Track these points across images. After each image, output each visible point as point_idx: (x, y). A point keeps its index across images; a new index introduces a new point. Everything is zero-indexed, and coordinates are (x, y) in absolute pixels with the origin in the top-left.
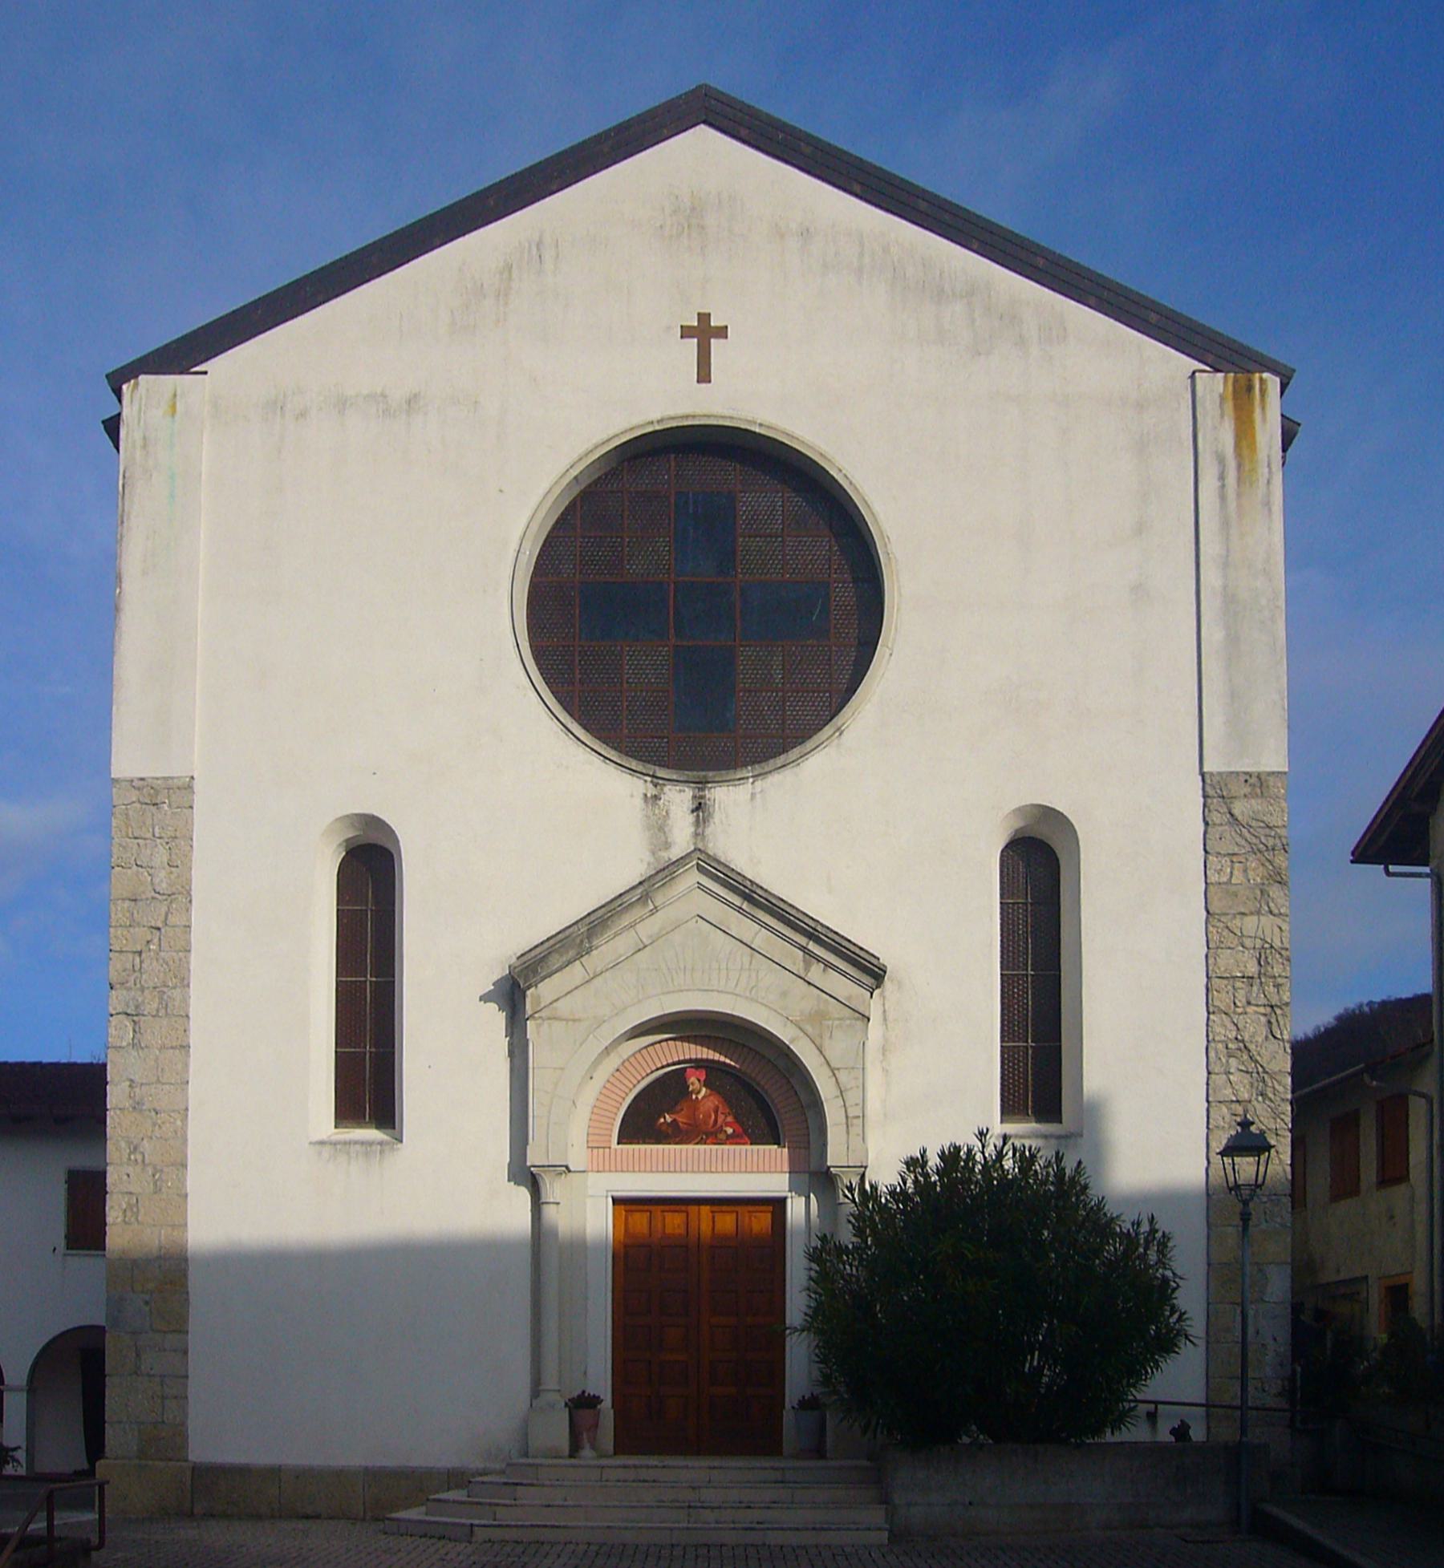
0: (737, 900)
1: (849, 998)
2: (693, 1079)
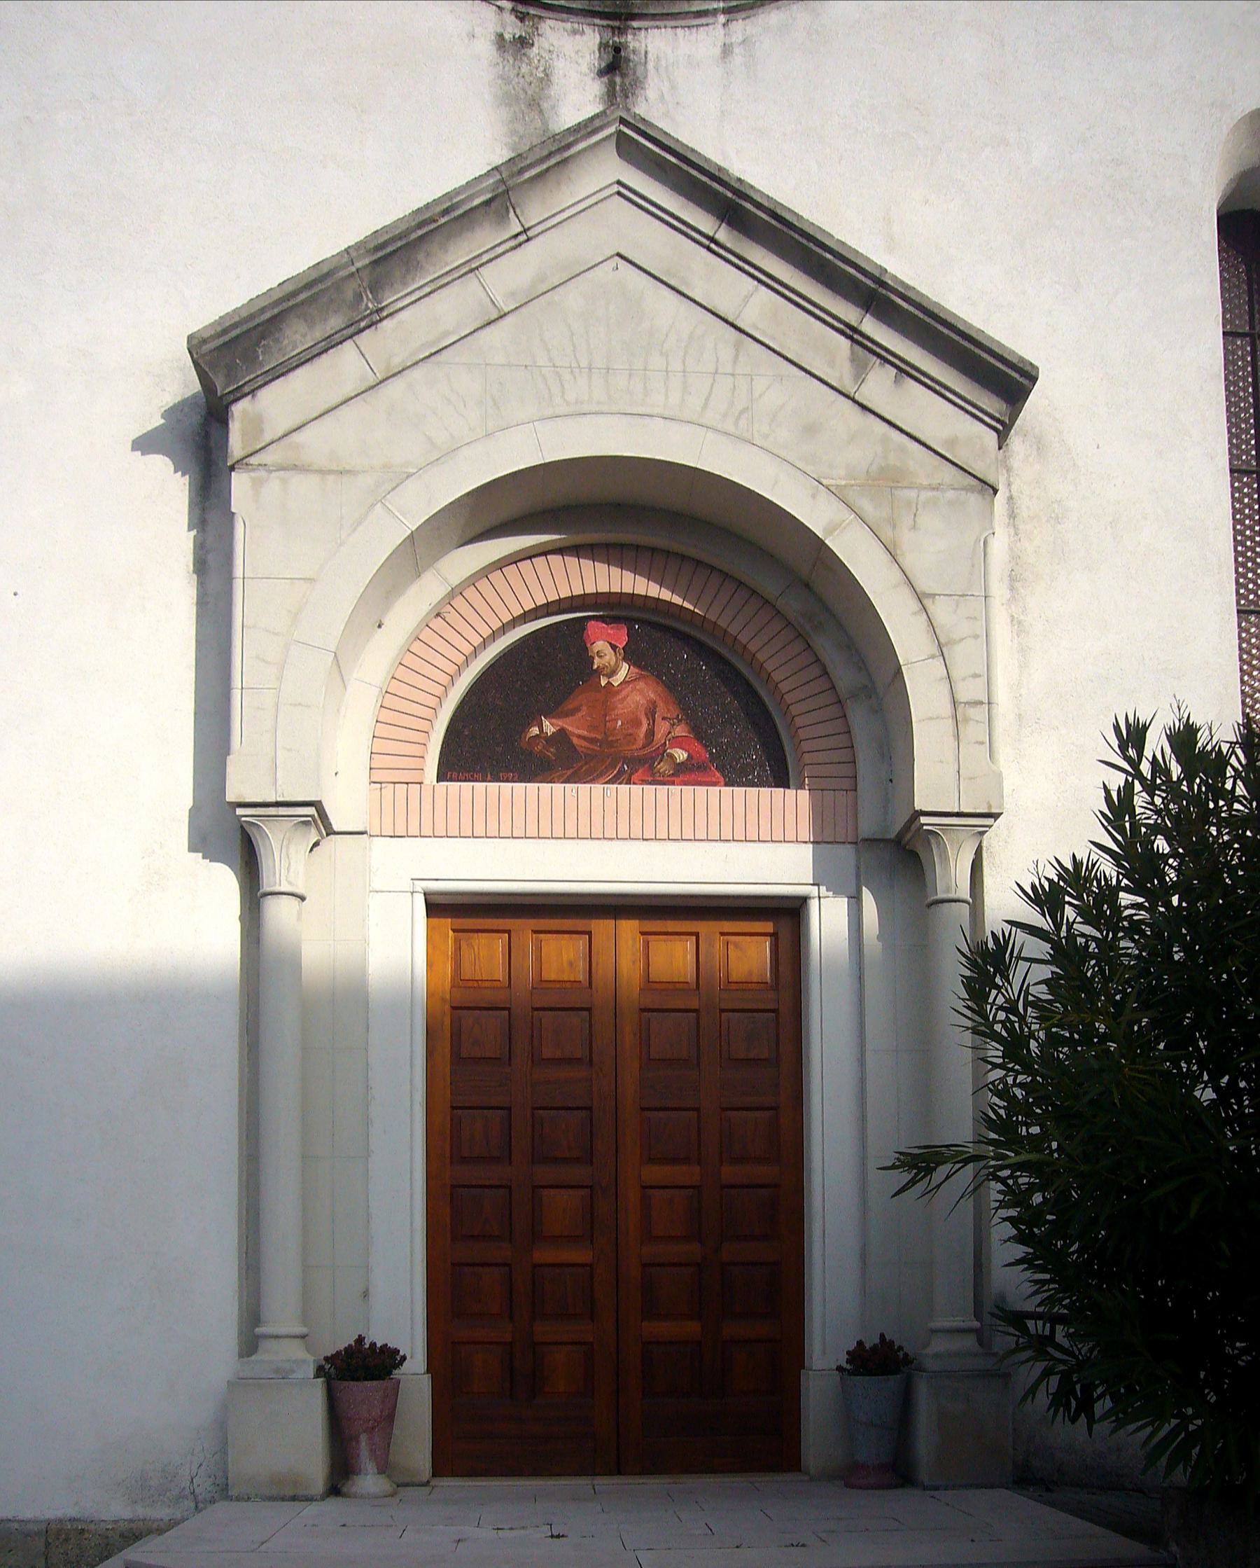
0: (704, 222)
1: (952, 442)
2: (600, 645)
